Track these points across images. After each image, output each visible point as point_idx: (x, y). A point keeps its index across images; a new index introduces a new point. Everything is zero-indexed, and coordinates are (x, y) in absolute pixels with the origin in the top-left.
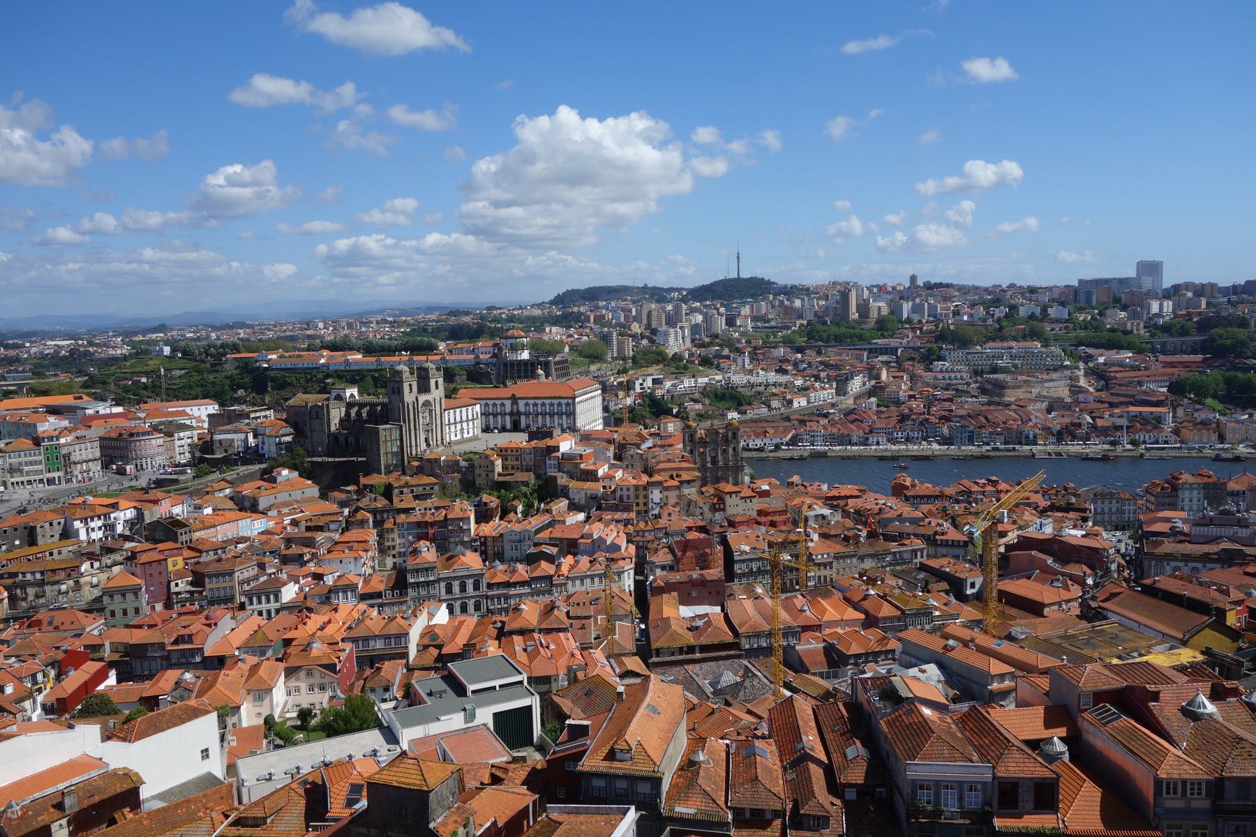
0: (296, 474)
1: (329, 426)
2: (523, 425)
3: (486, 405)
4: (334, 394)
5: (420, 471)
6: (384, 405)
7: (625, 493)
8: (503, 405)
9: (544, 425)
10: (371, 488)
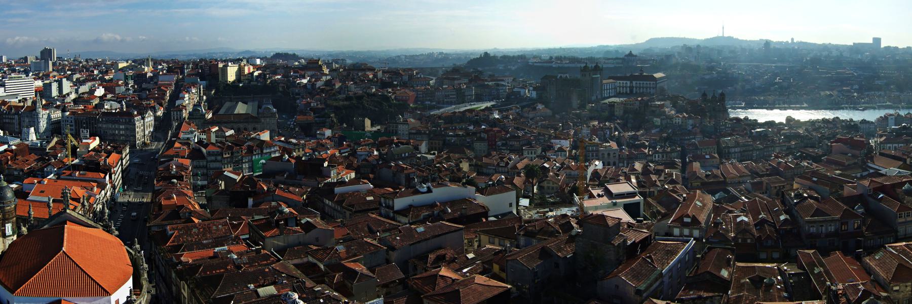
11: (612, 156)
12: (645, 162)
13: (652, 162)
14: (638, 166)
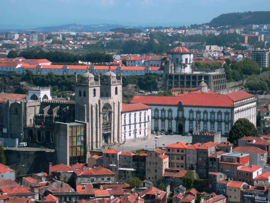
1: (25, 121)
2: (187, 129)
3: (156, 110)
4: (30, 94)
5: (99, 163)
6: (72, 106)
8: (170, 111)
9: (205, 130)
10: (57, 175)
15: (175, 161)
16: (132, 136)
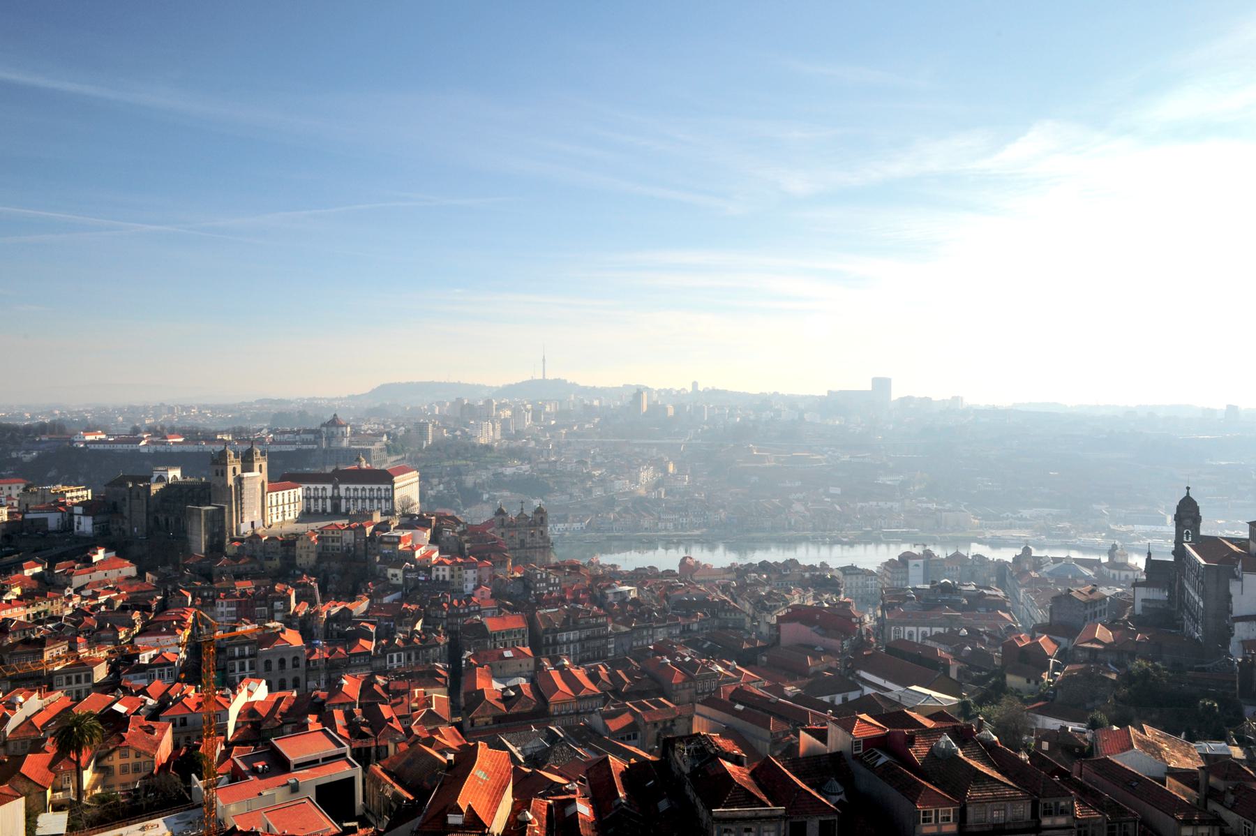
0: (113, 554)
2: (343, 510)
3: (308, 489)
4: (156, 476)
7: (441, 573)
8: (324, 489)
11: (289, 664)
12: (363, 674)
13: (383, 673)
14: (350, 685)
15: (330, 544)
16: (280, 519)
